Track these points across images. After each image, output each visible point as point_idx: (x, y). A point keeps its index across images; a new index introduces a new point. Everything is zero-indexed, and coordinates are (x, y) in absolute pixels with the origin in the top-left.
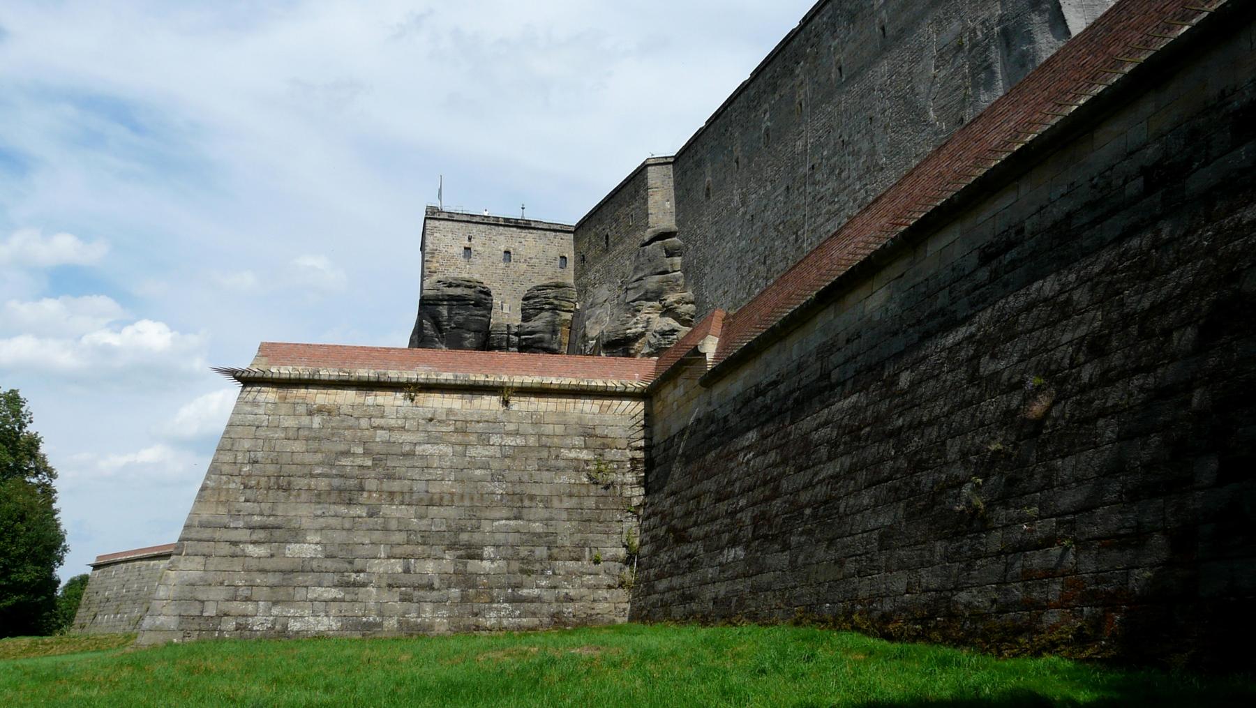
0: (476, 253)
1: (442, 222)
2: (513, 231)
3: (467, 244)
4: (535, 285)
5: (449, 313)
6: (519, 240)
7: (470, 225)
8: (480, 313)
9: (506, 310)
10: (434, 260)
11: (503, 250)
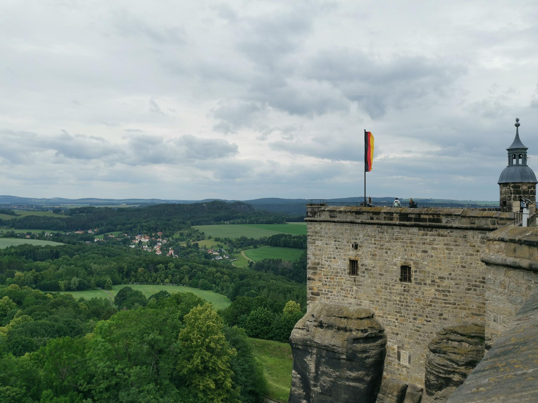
0: (364, 268)
1: (323, 225)
2: (413, 234)
3: (352, 254)
4: (448, 325)
5: (317, 368)
6: (423, 247)
7: (357, 228)
8: (354, 374)
9: (404, 361)
10: (317, 278)
11: (399, 265)
